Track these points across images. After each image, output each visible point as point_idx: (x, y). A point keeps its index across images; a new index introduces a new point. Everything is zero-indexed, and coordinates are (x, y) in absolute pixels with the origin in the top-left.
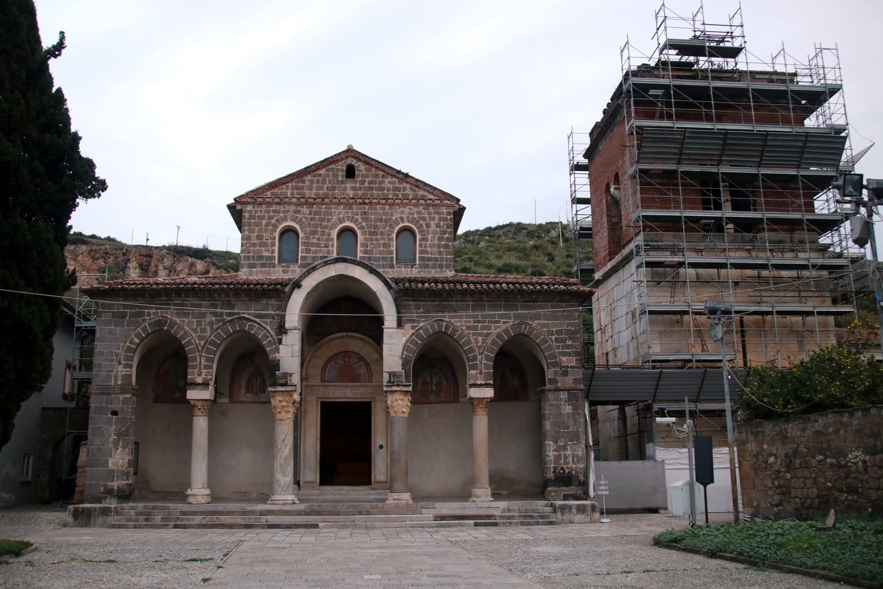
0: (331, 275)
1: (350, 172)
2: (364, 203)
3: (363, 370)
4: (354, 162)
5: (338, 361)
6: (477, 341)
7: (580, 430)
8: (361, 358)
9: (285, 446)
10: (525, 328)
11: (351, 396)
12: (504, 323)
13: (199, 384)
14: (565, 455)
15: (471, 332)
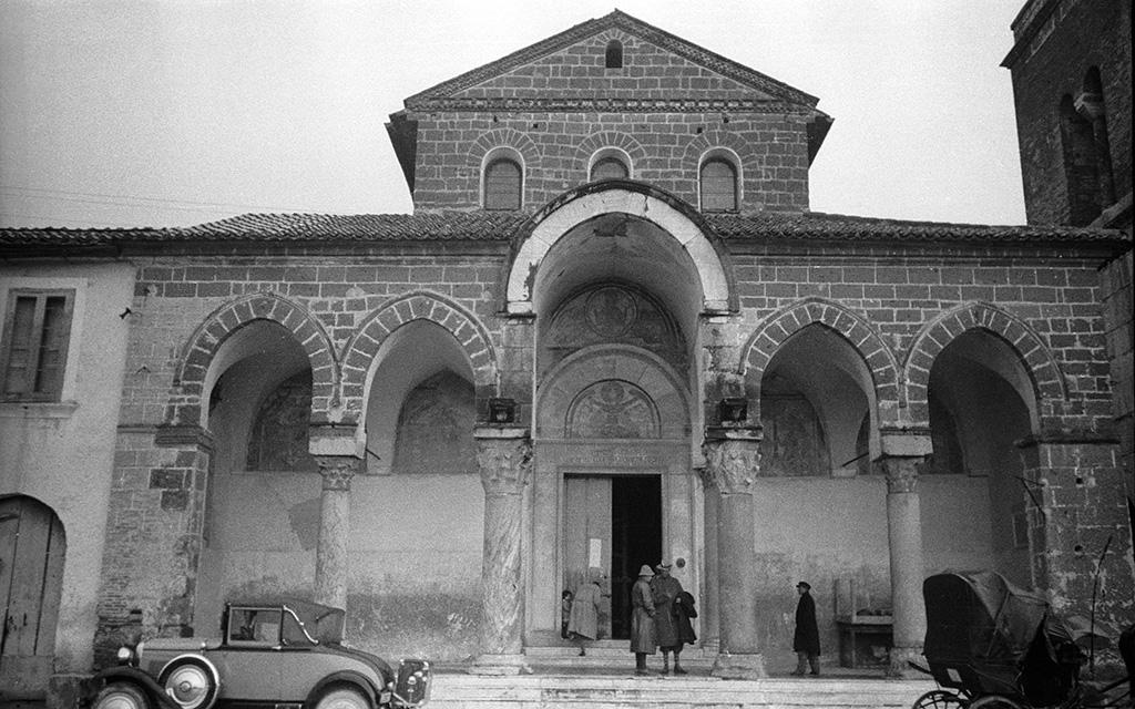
1: (614, 58)
6: (891, 343)
8: (643, 394)
9: (507, 551)
10: (989, 317)
12: (944, 306)
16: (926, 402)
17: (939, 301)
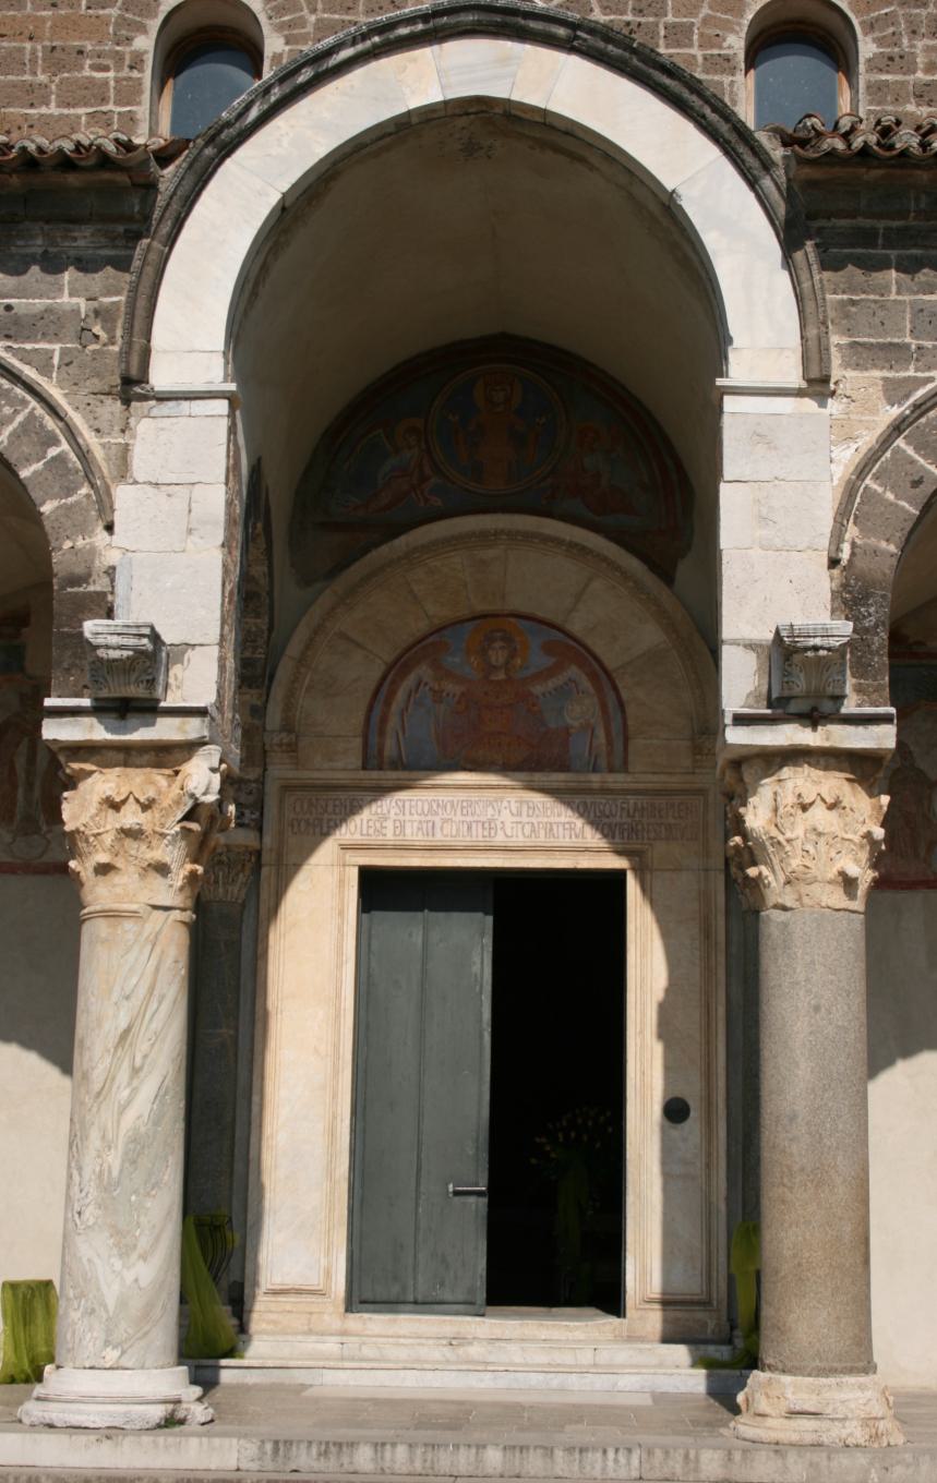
0: (415, 102)
3: (580, 711)
5: (453, 660)
8: (570, 649)
11: (519, 840)
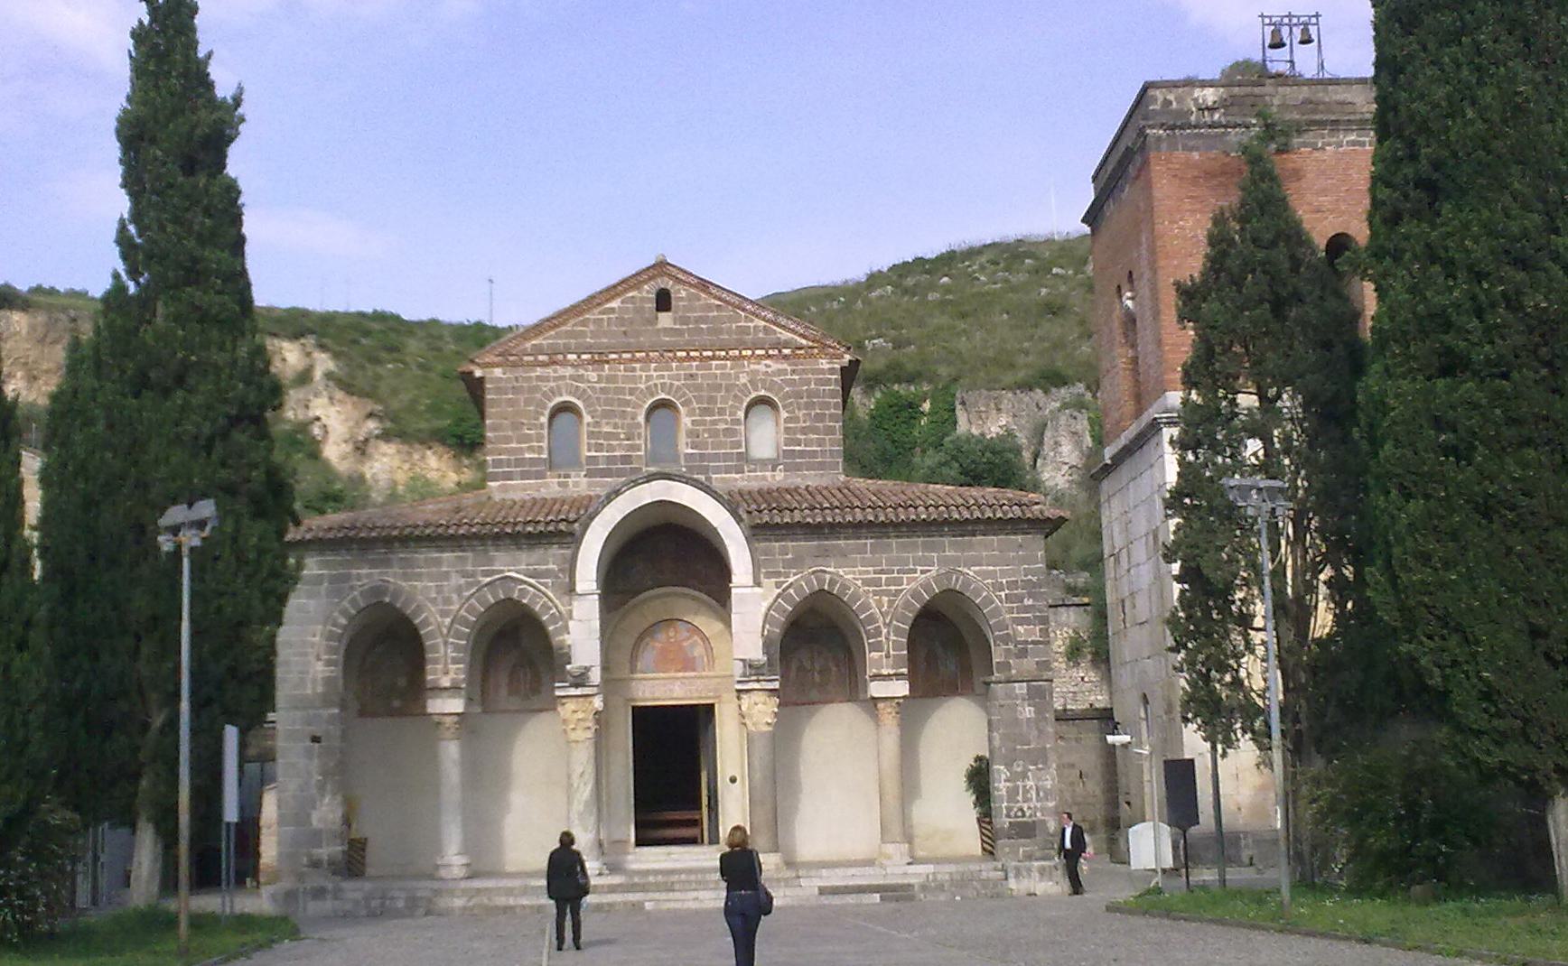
2: (689, 358)
4: (669, 284)
7: (1048, 746)
10: (957, 580)
12: (922, 572)
13: (446, 689)
14: (1024, 787)
15: (871, 589)
16: (905, 652)
17: (919, 568)
